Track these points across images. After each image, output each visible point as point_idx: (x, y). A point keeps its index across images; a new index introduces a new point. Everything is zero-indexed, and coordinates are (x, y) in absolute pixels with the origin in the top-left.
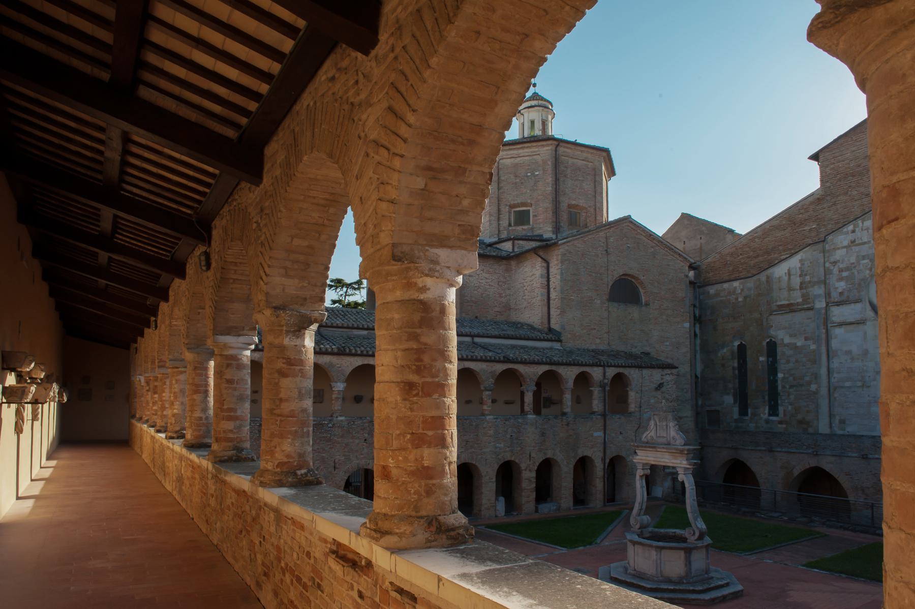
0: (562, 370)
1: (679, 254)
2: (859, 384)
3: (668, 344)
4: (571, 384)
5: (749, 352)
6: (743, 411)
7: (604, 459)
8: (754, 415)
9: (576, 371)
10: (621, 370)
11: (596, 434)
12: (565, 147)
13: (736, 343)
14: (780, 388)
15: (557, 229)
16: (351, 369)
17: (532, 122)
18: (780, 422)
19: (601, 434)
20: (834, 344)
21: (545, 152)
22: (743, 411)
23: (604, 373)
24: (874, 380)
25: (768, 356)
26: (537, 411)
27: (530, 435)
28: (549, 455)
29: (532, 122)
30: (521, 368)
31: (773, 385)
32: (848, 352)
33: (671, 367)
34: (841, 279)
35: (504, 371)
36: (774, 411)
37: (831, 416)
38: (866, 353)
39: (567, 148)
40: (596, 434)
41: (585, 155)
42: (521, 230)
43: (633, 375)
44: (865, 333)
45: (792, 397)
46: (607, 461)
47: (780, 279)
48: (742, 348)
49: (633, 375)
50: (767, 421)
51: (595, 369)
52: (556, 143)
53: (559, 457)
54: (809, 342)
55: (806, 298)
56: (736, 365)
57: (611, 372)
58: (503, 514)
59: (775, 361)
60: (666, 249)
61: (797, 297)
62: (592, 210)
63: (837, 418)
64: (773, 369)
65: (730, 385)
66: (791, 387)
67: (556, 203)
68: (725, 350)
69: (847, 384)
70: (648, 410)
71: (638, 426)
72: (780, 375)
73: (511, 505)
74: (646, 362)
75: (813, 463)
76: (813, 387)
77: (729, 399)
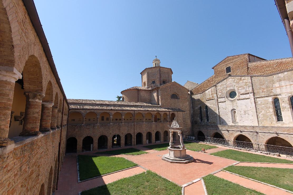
0: (160, 112)
2: (225, 114)
5: (202, 108)
6: (202, 121)
8: (204, 121)
9: (164, 112)
10: (173, 112)
13: (199, 107)
14: (209, 115)
15: (161, 85)
16: (114, 113)
17: (156, 64)
18: (210, 123)
20: (219, 106)
21: (158, 69)
22: (202, 121)
24: (229, 113)
25: (206, 109)
26: (155, 121)
27: (154, 126)
28: (158, 130)
29: (156, 64)
30: (151, 112)
31: (207, 115)
32: (222, 108)
33: (185, 111)
34: (220, 92)
35: (147, 113)
36: (208, 120)
37: (220, 121)
38: (226, 108)
42: (153, 85)
44: (226, 104)
45: (211, 117)
47: (207, 93)
48: (200, 107)
49: (176, 113)
50: (206, 123)
53: (160, 131)
54: (214, 106)
55: (213, 97)
56: (199, 111)
57: (171, 113)
58: (148, 143)
59: (207, 110)
61: (211, 97)
62: (168, 80)
63: (221, 122)
64: (207, 112)
65: (199, 115)
66: (211, 115)
67: (160, 79)
68: (197, 108)
69: (223, 114)
72: (209, 113)
73: (150, 141)
74: (179, 110)
75: (216, 131)
76: (216, 115)
77: (198, 118)
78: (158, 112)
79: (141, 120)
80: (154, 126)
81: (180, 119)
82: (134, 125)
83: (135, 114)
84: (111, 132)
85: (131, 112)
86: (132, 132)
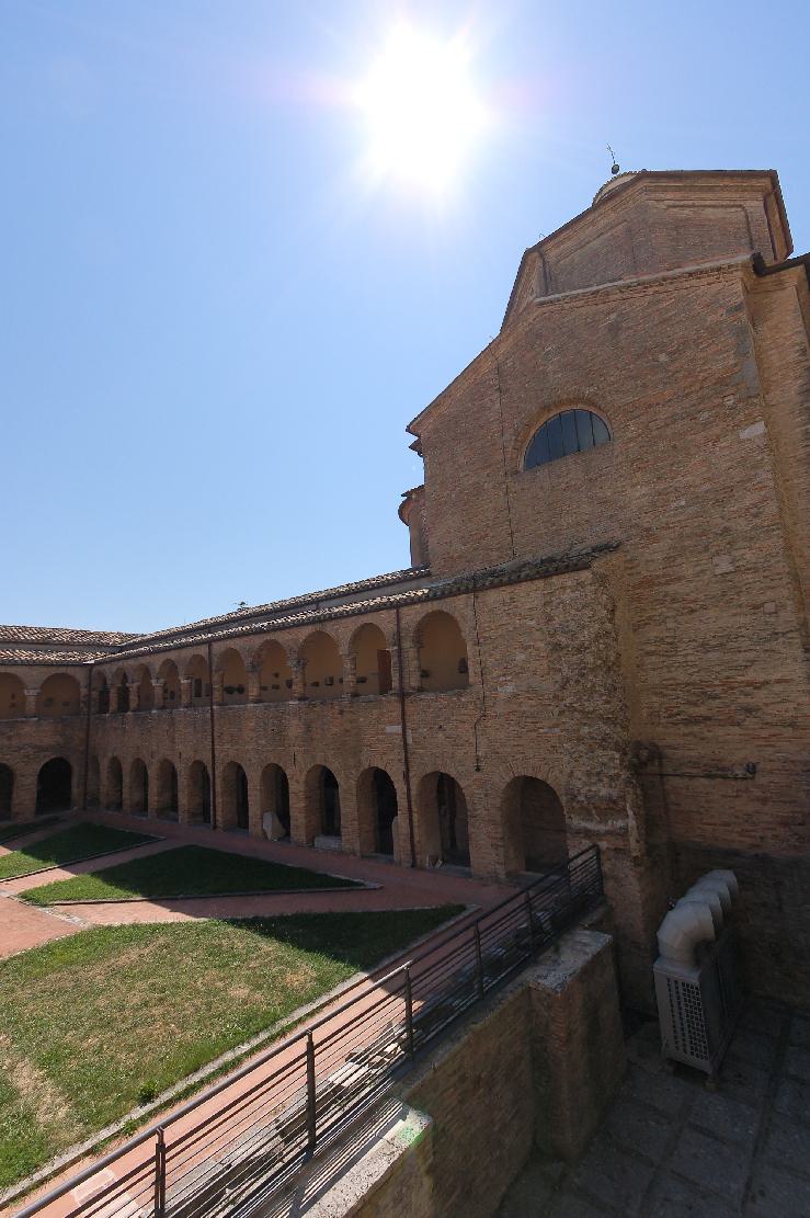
0: (329, 628)
1: (690, 274)
3: (683, 503)
4: (343, 649)
7: (406, 777)
9: (351, 626)
11: (389, 729)
12: (558, 245)
19: (398, 729)
23: (398, 620)
27: (294, 729)
28: (319, 761)
30: (279, 637)
39: (562, 242)
40: (389, 729)
41: (602, 223)
43: (459, 606)
46: (414, 782)
51: (384, 614)
52: (536, 254)
53: (334, 766)
60: (650, 291)
70: (509, 678)
71: (478, 714)
78: (318, 627)
79: (317, 684)
80: (294, 729)
81: (521, 657)
82: (212, 716)
83: (215, 659)
84: (154, 748)
85: (203, 650)
86: (206, 757)
